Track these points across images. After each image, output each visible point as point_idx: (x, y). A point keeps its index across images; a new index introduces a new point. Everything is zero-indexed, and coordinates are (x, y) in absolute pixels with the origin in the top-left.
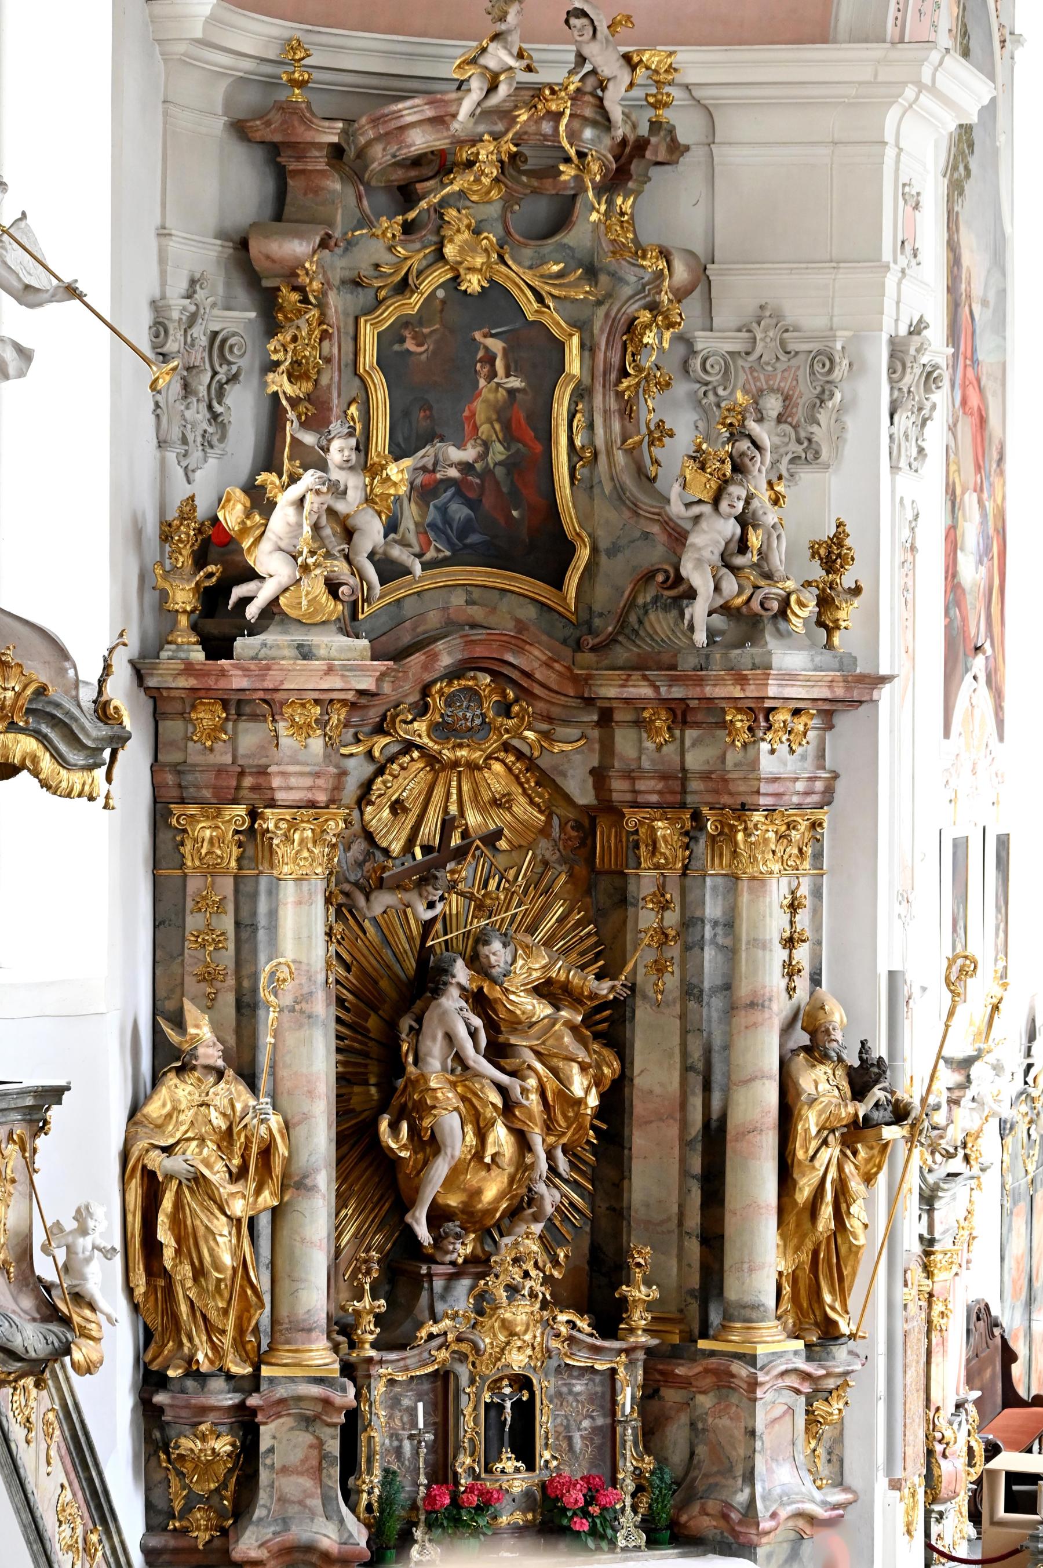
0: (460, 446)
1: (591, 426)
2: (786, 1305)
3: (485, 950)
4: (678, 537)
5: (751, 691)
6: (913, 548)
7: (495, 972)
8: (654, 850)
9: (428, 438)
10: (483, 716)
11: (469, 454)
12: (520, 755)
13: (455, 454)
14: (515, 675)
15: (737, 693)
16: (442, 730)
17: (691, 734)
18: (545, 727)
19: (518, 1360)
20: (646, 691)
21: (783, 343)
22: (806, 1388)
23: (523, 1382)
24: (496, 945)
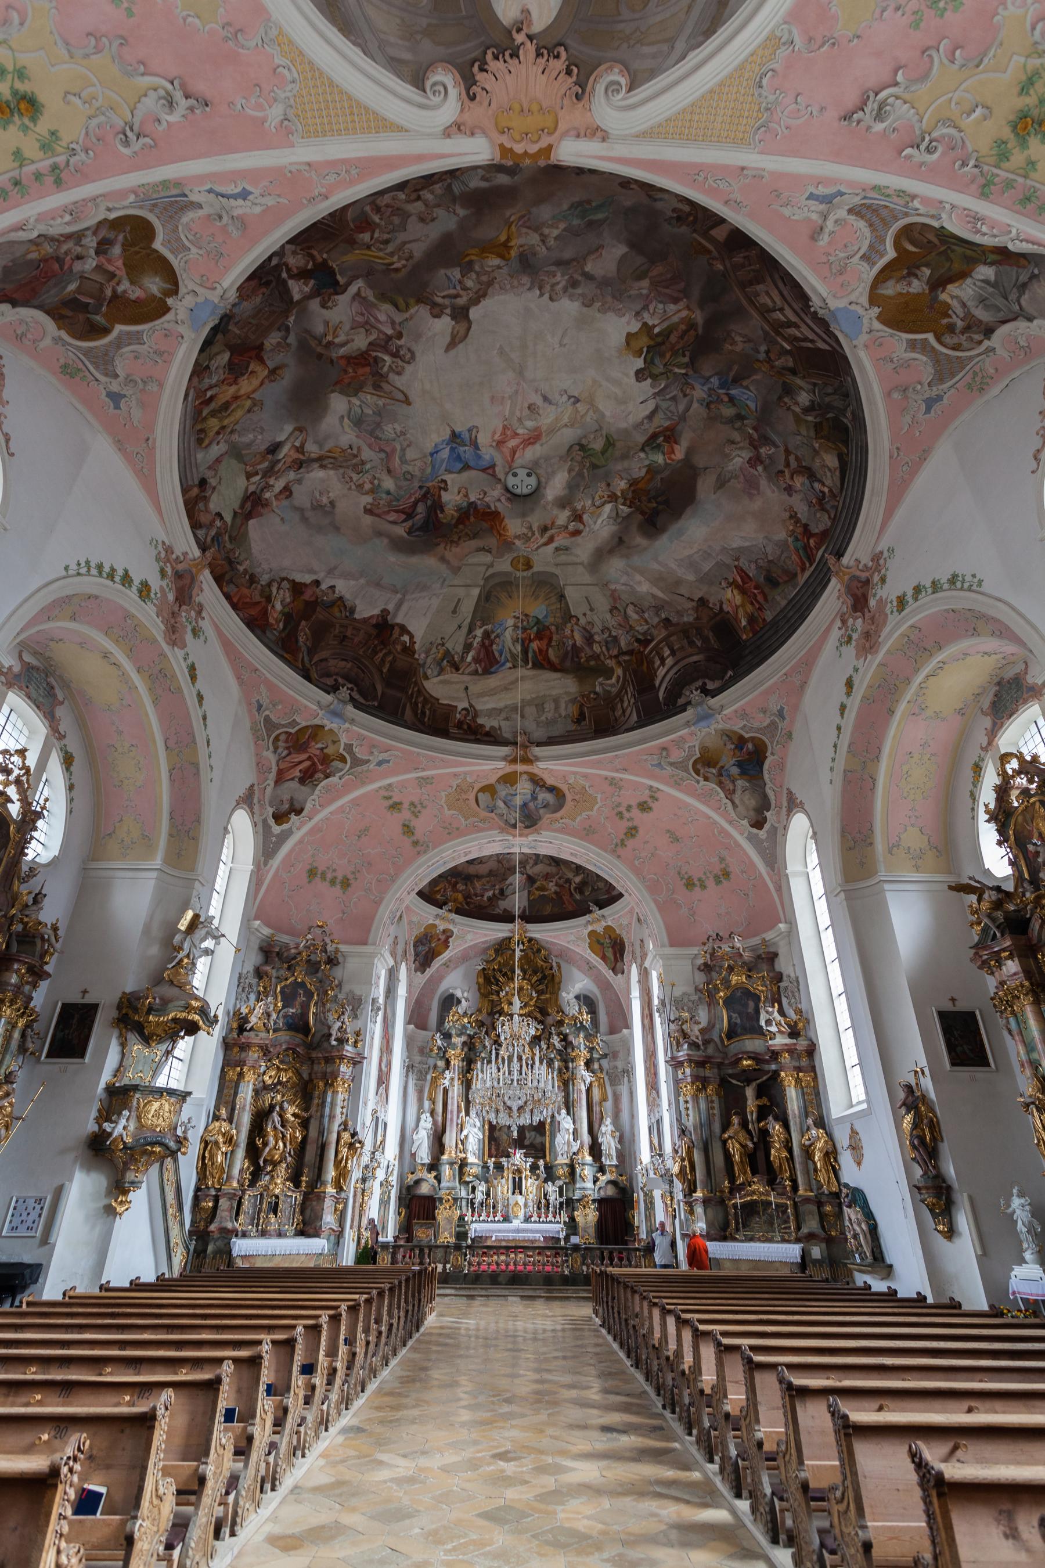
4: (329, 1028)
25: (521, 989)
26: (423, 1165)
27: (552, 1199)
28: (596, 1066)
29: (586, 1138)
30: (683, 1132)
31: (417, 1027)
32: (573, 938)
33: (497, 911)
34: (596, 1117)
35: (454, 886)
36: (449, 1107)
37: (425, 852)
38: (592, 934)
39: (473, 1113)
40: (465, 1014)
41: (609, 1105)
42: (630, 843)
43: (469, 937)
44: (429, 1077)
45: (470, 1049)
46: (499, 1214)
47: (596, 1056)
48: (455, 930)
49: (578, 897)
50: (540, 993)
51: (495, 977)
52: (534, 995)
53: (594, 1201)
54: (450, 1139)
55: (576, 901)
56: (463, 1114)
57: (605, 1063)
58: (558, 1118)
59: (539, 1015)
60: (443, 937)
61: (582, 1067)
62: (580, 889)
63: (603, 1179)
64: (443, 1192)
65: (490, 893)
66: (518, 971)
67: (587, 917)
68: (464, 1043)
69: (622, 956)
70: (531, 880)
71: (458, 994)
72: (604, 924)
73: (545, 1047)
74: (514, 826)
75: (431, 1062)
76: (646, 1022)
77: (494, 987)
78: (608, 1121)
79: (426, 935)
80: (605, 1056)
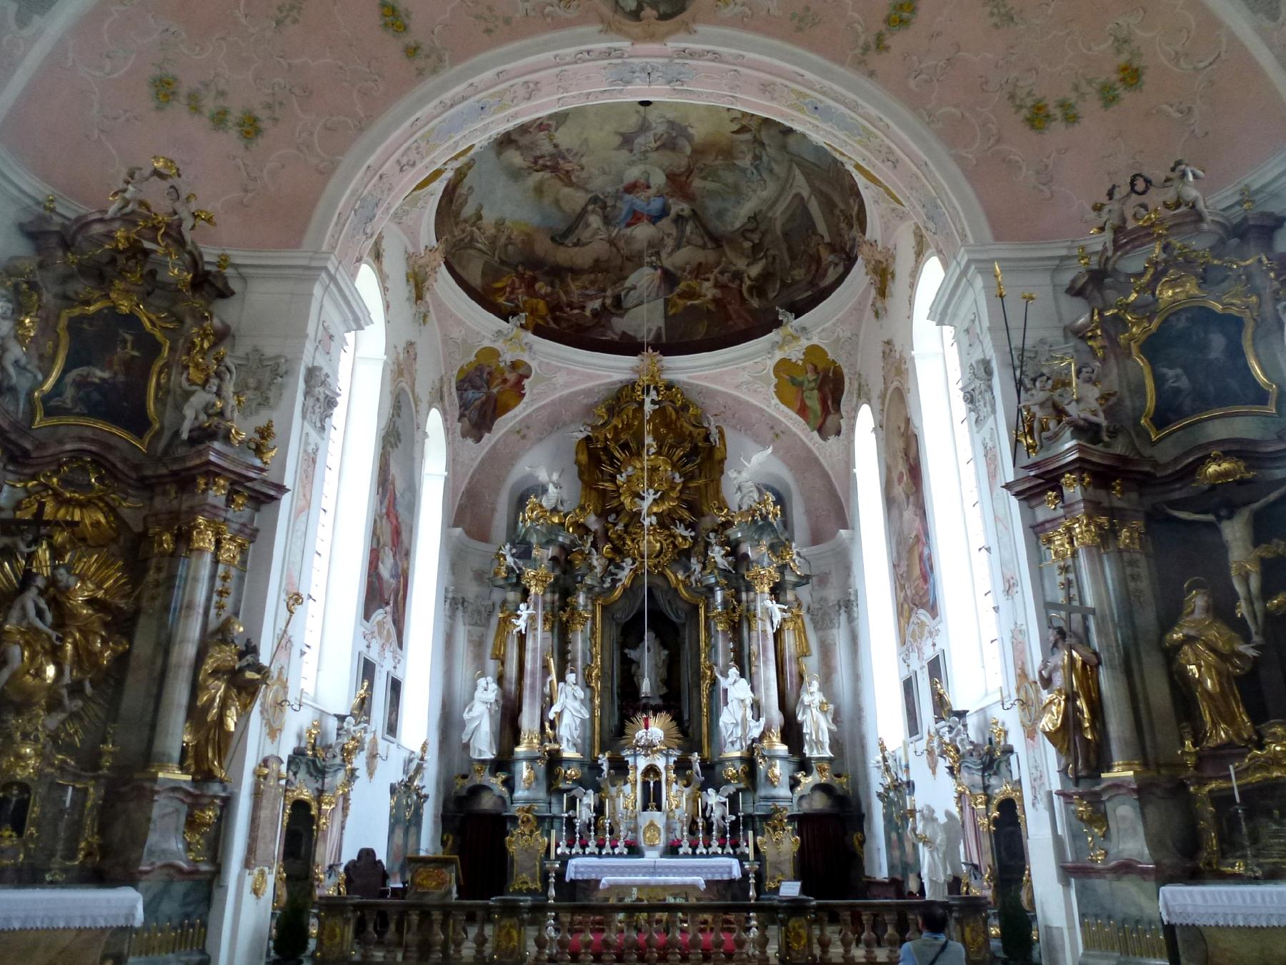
0: (103, 370)
1: (169, 380)
2: (190, 761)
3: (56, 572)
5: (203, 459)
6: (314, 461)
7: (61, 584)
8: (161, 544)
9: (88, 363)
10: (90, 481)
11: (106, 375)
12: (107, 504)
13: (99, 373)
14: (107, 464)
15: (197, 461)
16: (65, 482)
17: (185, 497)
18: (125, 496)
19: (20, 774)
20: (164, 471)
21: (261, 360)
22: (188, 800)
23: (24, 787)
24: (62, 571)
25: (654, 469)
26: (483, 762)
27: (716, 815)
28: (790, 596)
29: (777, 717)
30: (1060, 636)
31: (468, 532)
32: (745, 377)
33: (610, 336)
34: (790, 681)
35: (530, 284)
36: (528, 666)
37: (435, 71)
38: (783, 367)
39: (571, 677)
40: (554, 510)
41: (812, 663)
42: (897, 41)
43: (560, 379)
44: (494, 622)
45: (564, 572)
46: (621, 844)
47: (790, 578)
48: (533, 364)
49: (755, 303)
50: (688, 477)
51: (606, 449)
52: (678, 479)
53: (792, 818)
54: (529, 720)
55: (752, 312)
56: (553, 677)
57: (804, 593)
58: (724, 683)
59: (686, 515)
60: (512, 377)
61: (767, 596)
62: (759, 288)
63: (808, 781)
64: (518, 805)
65: (596, 304)
66: (649, 440)
67: (773, 336)
68: (554, 559)
69: (837, 402)
70: (669, 279)
71: (543, 476)
72: (804, 343)
73: (698, 567)
74: (636, 15)
75: (497, 596)
76: (899, 491)
77: (609, 469)
78: (815, 686)
79: (479, 368)
80: (804, 580)
